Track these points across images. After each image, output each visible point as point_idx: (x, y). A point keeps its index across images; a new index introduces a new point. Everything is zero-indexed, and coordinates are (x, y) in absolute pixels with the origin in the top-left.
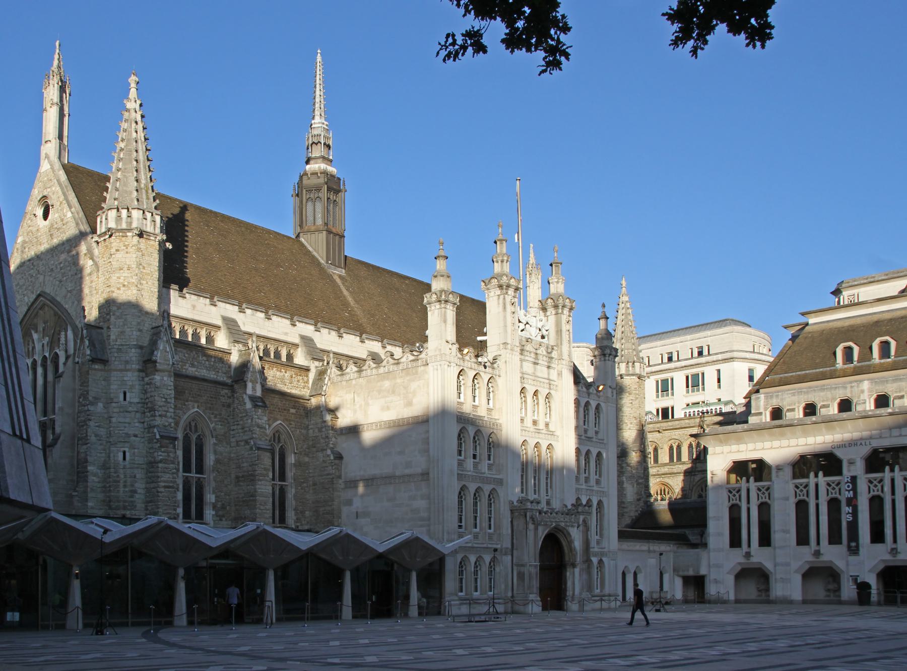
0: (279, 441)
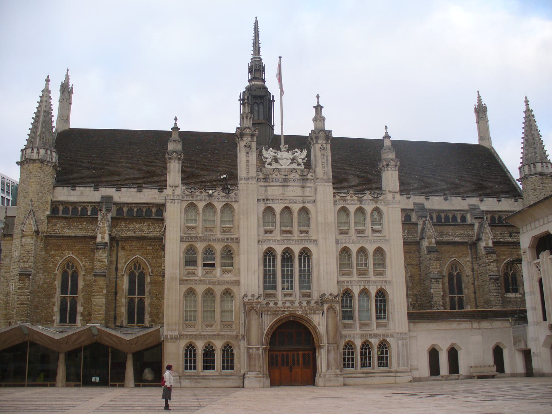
0: (139, 269)
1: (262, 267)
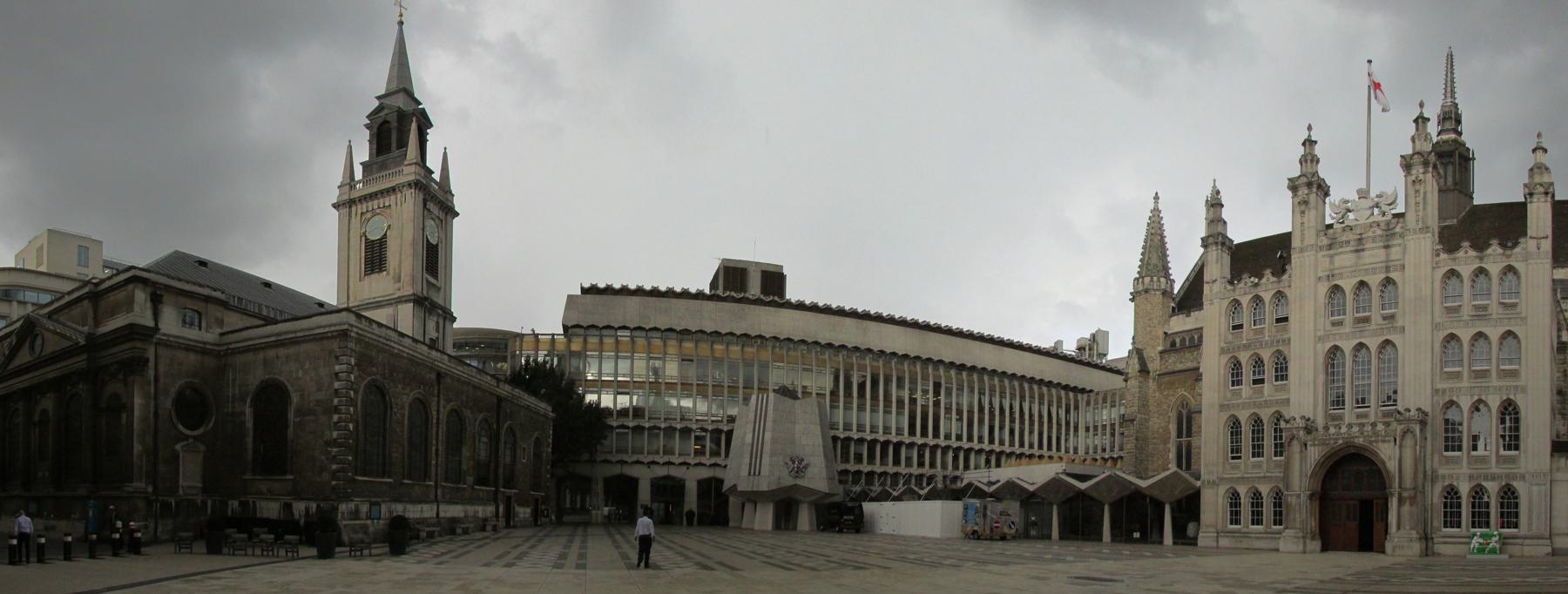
1: (1321, 378)
